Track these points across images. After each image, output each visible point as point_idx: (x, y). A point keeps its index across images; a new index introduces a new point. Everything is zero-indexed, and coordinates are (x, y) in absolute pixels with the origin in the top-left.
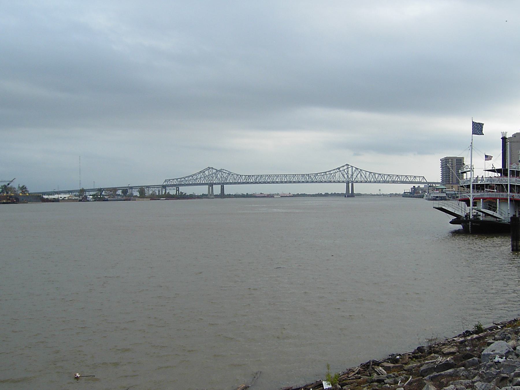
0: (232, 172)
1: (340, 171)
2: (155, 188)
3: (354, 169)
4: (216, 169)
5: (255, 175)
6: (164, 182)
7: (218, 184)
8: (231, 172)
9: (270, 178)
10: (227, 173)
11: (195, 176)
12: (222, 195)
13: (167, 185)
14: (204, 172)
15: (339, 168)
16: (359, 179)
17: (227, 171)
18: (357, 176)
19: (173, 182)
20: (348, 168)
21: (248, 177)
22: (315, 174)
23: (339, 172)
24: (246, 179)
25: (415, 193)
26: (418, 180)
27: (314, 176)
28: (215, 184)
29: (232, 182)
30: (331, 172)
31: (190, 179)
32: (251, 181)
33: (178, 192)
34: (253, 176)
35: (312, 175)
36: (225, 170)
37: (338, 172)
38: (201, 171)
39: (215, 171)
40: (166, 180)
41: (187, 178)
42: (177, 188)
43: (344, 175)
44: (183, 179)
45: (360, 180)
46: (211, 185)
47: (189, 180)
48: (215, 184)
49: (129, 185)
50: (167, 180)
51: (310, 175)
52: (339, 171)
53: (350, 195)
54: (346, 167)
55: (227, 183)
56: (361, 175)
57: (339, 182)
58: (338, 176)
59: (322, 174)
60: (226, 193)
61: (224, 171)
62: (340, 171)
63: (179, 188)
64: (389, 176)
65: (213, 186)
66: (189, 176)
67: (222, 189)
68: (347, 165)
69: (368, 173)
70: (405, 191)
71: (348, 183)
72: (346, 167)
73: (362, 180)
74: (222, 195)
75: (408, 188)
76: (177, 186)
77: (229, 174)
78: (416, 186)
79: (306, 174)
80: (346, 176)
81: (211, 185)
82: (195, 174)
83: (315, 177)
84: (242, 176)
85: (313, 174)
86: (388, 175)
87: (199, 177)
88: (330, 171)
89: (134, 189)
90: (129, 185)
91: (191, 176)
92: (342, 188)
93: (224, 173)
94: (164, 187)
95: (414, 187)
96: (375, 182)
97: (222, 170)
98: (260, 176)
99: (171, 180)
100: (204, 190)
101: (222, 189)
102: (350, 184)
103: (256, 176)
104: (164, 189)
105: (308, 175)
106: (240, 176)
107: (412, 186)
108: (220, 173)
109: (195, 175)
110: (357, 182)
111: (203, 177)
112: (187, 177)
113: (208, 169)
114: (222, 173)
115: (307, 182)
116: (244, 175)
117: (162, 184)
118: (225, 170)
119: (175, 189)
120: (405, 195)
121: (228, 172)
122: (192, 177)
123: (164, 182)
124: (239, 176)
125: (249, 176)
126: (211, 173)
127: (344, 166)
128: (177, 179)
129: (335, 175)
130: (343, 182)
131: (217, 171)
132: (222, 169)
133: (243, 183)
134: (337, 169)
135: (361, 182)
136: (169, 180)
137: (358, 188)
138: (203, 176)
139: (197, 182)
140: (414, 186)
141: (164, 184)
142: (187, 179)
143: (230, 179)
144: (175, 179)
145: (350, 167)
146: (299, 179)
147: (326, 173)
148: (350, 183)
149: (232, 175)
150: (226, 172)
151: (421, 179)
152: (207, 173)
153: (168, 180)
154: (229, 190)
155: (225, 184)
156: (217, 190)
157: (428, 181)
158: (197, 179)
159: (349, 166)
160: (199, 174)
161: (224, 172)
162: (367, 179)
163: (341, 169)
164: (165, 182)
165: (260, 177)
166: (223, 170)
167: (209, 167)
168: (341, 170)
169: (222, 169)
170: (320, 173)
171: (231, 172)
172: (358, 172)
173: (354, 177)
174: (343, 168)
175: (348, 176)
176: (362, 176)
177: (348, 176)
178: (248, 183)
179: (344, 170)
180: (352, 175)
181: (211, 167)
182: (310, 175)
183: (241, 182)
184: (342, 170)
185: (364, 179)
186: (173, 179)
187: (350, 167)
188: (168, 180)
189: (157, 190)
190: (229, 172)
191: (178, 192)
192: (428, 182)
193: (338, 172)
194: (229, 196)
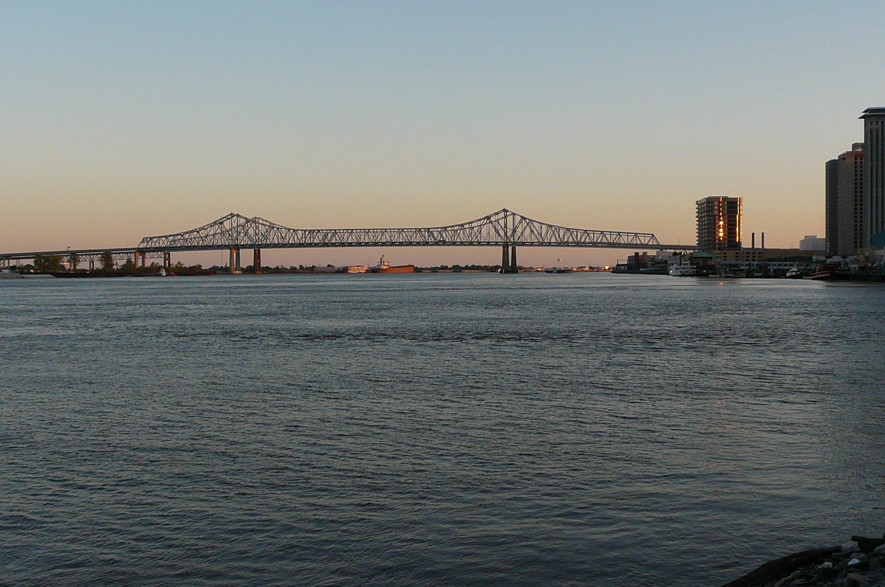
1: (491, 222)
2: (121, 254)
3: (518, 219)
4: (246, 218)
5: (322, 230)
6: (141, 243)
7: (250, 246)
10: (267, 226)
11: (203, 231)
12: (256, 269)
13: (146, 248)
14: (222, 223)
15: (488, 218)
16: (527, 236)
17: (266, 221)
19: (159, 243)
20: (506, 217)
21: (310, 232)
22: (442, 228)
24: (305, 237)
25: (636, 266)
26: (645, 240)
27: (440, 232)
28: (244, 247)
30: (473, 225)
32: (290, 242)
33: (167, 261)
34: (319, 231)
35: (436, 230)
36: (263, 220)
37: (486, 223)
38: (216, 221)
39: (244, 221)
40: (144, 238)
44: (179, 237)
45: (529, 241)
48: (244, 247)
50: (147, 238)
51: (430, 230)
52: (488, 221)
53: (510, 268)
55: (267, 246)
56: (532, 231)
57: (488, 244)
58: (487, 233)
59: (456, 228)
60: (263, 265)
61: (261, 221)
62: (491, 222)
63: (169, 254)
65: (239, 250)
66: (192, 232)
67: (257, 256)
68: (505, 211)
69: (544, 228)
70: (619, 263)
71: (505, 246)
72: (502, 215)
74: (256, 269)
75: (623, 256)
76: (166, 250)
77: (273, 228)
78: (641, 252)
79: (425, 229)
80: (502, 233)
81: (237, 248)
83: (442, 235)
84: (297, 230)
85: (437, 228)
88: (471, 223)
92: (494, 256)
93: (260, 225)
94: (142, 252)
95: (637, 254)
96: (559, 244)
98: (333, 231)
99: (156, 239)
100: (221, 258)
101: (257, 256)
102: (510, 248)
104: (141, 257)
105: (428, 229)
106: (294, 231)
107: (632, 252)
108: (253, 225)
109: (203, 229)
111: (218, 233)
112: (187, 233)
113: (230, 216)
114: (257, 225)
115: (426, 244)
116: (302, 230)
117: (136, 247)
118: (263, 220)
119: (161, 257)
120: (618, 270)
121: (269, 224)
122: (198, 232)
123: (141, 243)
124: (292, 231)
125: (310, 231)
126: (235, 225)
127: (497, 214)
128: (167, 237)
130: (497, 244)
131: (248, 221)
132: (257, 217)
133: (300, 245)
134: (484, 218)
135: (532, 244)
136: (151, 239)
138: (219, 231)
140: (635, 253)
141: (140, 247)
142: (187, 236)
144: (163, 237)
145: (509, 215)
146: (392, 238)
147: (463, 226)
148: (510, 245)
149: (278, 229)
150: (265, 223)
151: (647, 239)
152: (227, 225)
154: (269, 258)
155: (262, 248)
156: (247, 258)
157: (661, 244)
158: (206, 236)
159: (508, 213)
160: (212, 226)
161: (262, 224)
163: (493, 219)
164: (143, 241)
165: (333, 233)
166: (259, 218)
167: (231, 214)
169: (256, 218)
170: (452, 227)
171: (274, 224)
175: (506, 234)
176: (533, 232)
177: (506, 234)
178: (310, 245)
179: (498, 221)
180: (514, 231)
182: (430, 230)
184: (495, 221)
186: (159, 237)
187: (509, 215)
190: (270, 223)
191: (167, 261)
192: (662, 246)
193: (486, 223)
194: (268, 271)
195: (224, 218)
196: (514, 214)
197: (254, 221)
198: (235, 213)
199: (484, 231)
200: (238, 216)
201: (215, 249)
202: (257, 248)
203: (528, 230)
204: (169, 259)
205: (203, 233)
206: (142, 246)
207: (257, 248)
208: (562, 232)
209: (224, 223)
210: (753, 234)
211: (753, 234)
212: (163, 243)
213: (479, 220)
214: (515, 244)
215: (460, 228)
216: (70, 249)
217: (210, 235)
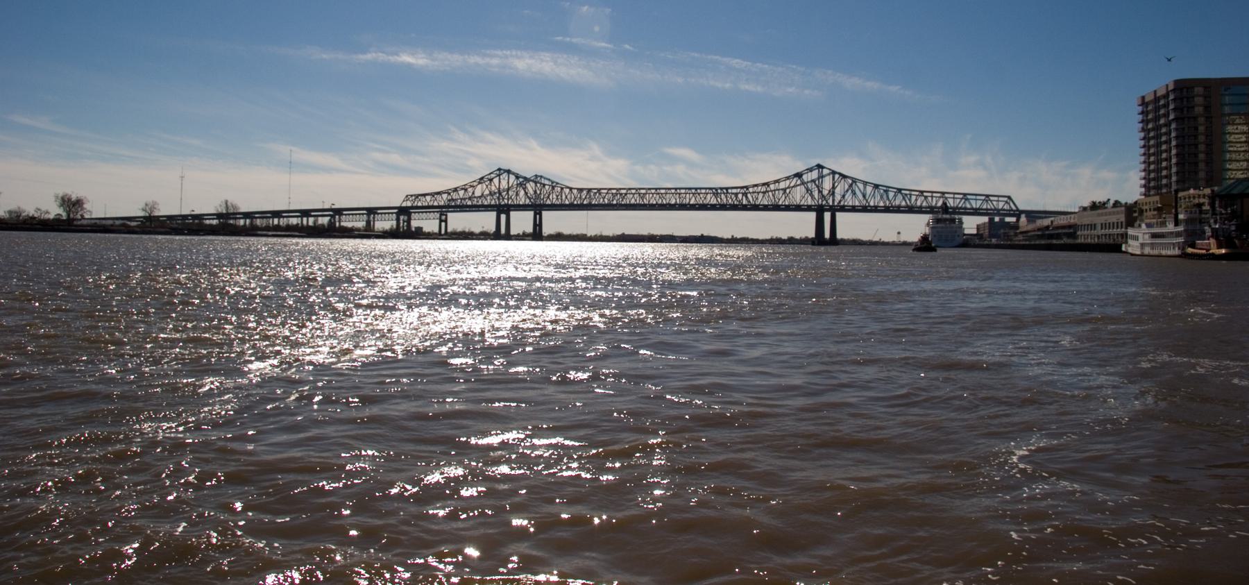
0: (560, 182)
6: (404, 201)
8: (557, 181)
13: (412, 207)
14: (491, 180)
15: (799, 175)
16: (849, 201)
17: (549, 180)
18: (843, 196)
20: (821, 177)
23: (798, 185)
29: (655, 202)
33: (443, 224)
36: (545, 178)
38: (482, 178)
40: (407, 196)
42: (441, 215)
43: (811, 192)
45: (850, 204)
49: (333, 204)
50: (412, 196)
52: (799, 182)
53: (823, 240)
54: (815, 174)
55: (553, 207)
56: (854, 193)
57: (798, 208)
58: (798, 195)
62: (803, 183)
63: (446, 215)
64: (902, 194)
68: (820, 167)
69: (869, 189)
71: (820, 210)
73: (857, 204)
74: (537, 235)
76: (443, 211)
80: (816, 194)
86: (898, 189)
87: (478, 193)
89: (346, 215)
90: (333, 204)
91: (462, 189)
92: (804, 225)
96: (887, 210)
97: (539, 178)
102: (827, 216)
103: (606, 191)
109: (471, 186)
110: (843, 209)
113: (498, 172)
117: (398, 205)
129: (790, 193)
130: (809, 208)
137: (849, 226)
143: (554, 199)
147: (768, 186)
148: (827, 210)
152: (496, 181)
159: (825, 172)
162: (867, 201)
163: (805, 177)
166: (541, 177)
167: (499, 169)
168: (806, 181)
169: (536, 176)
171: (557, 183)
172: (847, 187)
173: (838, 198)
174: (809, 174)
176: (855, 194)
179: (813, 181)
180: (832, 192)
181: (507, 169)
185: (860, 201)
187: (829, 174)
190: (553, 183)
191: (443, 224)
195: (492, 173)
196: (834, 173)
197: (536, 179)
200: (509, 172)
202: (538, 208)
203: (850, 191)
204: (446, 221)
206: (404, 205)
207: (538, 208)
208: (891, 195)
209: (494, 180)
212: (442, 200)
213: (788, 178)
214: (834, 210)
216: (333, 207)
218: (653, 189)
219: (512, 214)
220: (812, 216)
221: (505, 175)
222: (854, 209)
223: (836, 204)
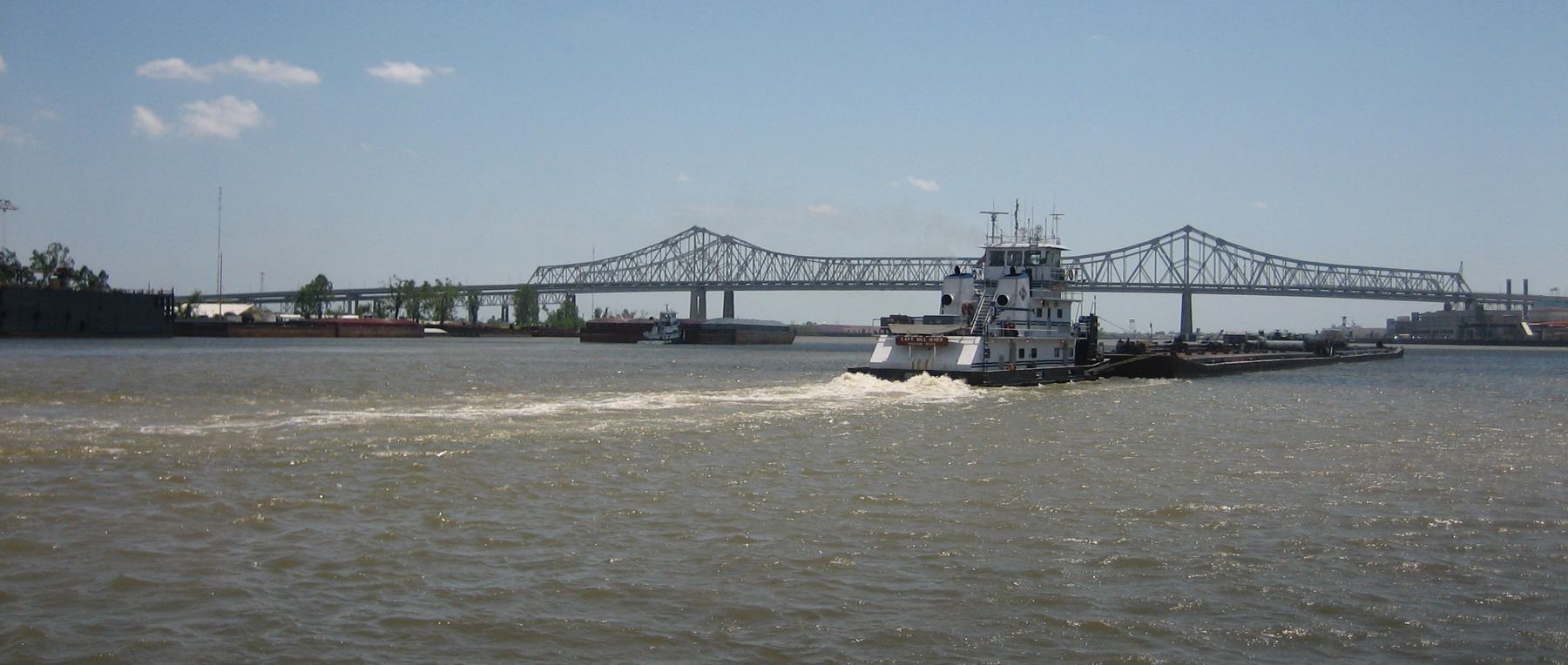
4: (718, 236)
9: (832, 268)
13: (540, 286)
28: (714, 286)
31: (596, 270)
32: (682, 280)
38: (668, 240)
40: (539, 268)
41: (616, 263)
46: (699, 290)
47: (594, 272)
48: (714, 286)
50: (544, 268)
55: (743, 286)
57: (1155, 288)
66: (623, 258)
76: (570, 290)
82: (630, 254)
99: (559, 270)
112: (614, 259)
128: (577, 266)
130: (1170, 289)
136: (550, 269)
139: (652, 276)
153: (546, 270)
154: (752, 308)
183: (662, 283)
188: (546, 270)
189: (498, 302)
197: (728, 240)
198: (701, 226)
199: (1149, 266)
200: (704, 231)
201: (650, 289)
205: (642, 260)
206: (535, 281)
210: (1526, 282)
211: (1526, 282)
212: (570, 277)
215: (904, 262)
217: (655, 264)
218: (869, 259)
219: (707, 292)
220: (1180, 296)
221: (700, 234)
222: (1219, 289)
223: (1190, 282)
